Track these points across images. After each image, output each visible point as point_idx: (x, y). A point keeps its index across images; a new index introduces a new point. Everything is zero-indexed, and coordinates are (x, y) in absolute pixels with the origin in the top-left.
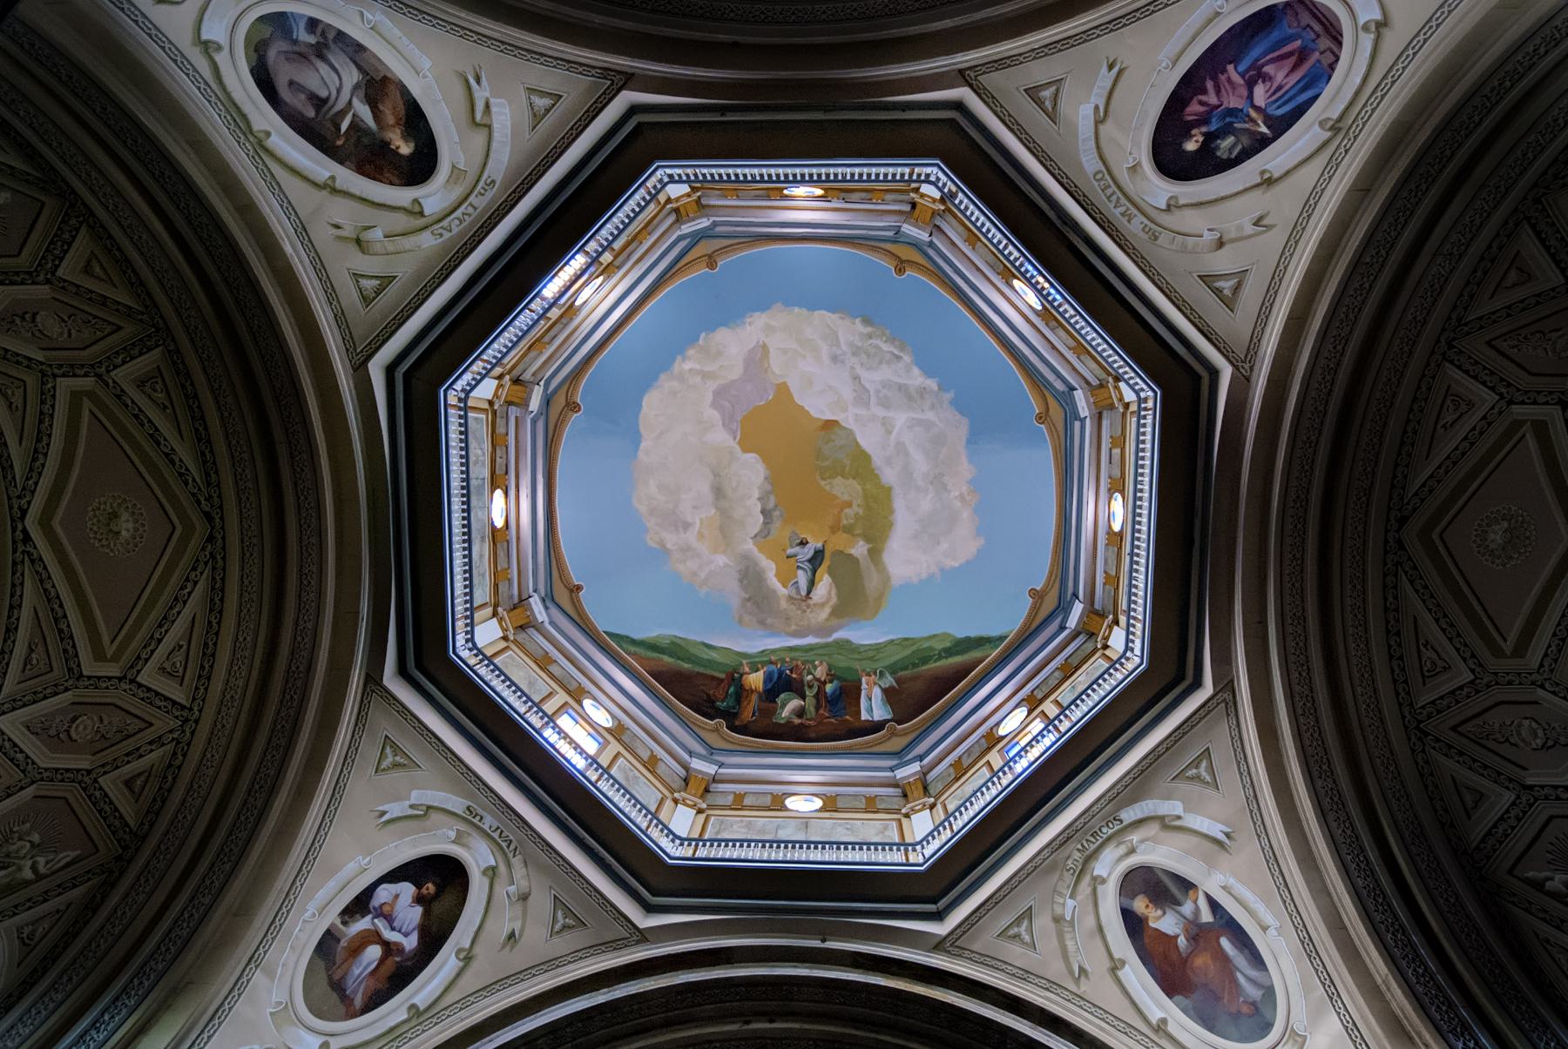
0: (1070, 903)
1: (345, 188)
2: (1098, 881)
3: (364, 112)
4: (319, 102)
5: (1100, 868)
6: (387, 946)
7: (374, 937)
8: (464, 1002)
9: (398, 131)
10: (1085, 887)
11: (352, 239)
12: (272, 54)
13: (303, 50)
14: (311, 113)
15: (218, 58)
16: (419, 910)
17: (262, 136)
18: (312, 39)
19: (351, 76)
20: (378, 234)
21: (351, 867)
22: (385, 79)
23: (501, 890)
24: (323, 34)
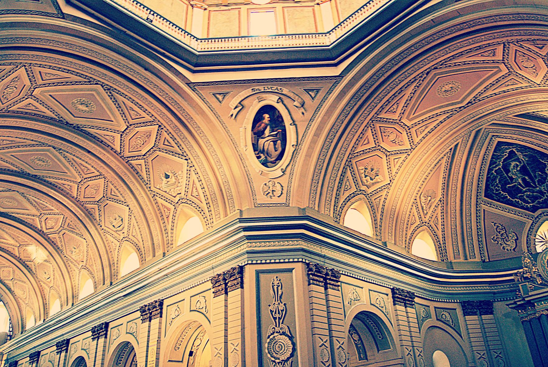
1: (291, 120)
3: (267, 132)
4: (275, 142)
9: (264, 121)
11: (304, 108)
12: (273, 159)
13: (266, 155)
14: (279, 142)
15: (284, 168)
17: (294, 146)
18: (262, 155)
19: (261, 141)
20: (296, 103)
22: (255, 134)
24: (258, 154)
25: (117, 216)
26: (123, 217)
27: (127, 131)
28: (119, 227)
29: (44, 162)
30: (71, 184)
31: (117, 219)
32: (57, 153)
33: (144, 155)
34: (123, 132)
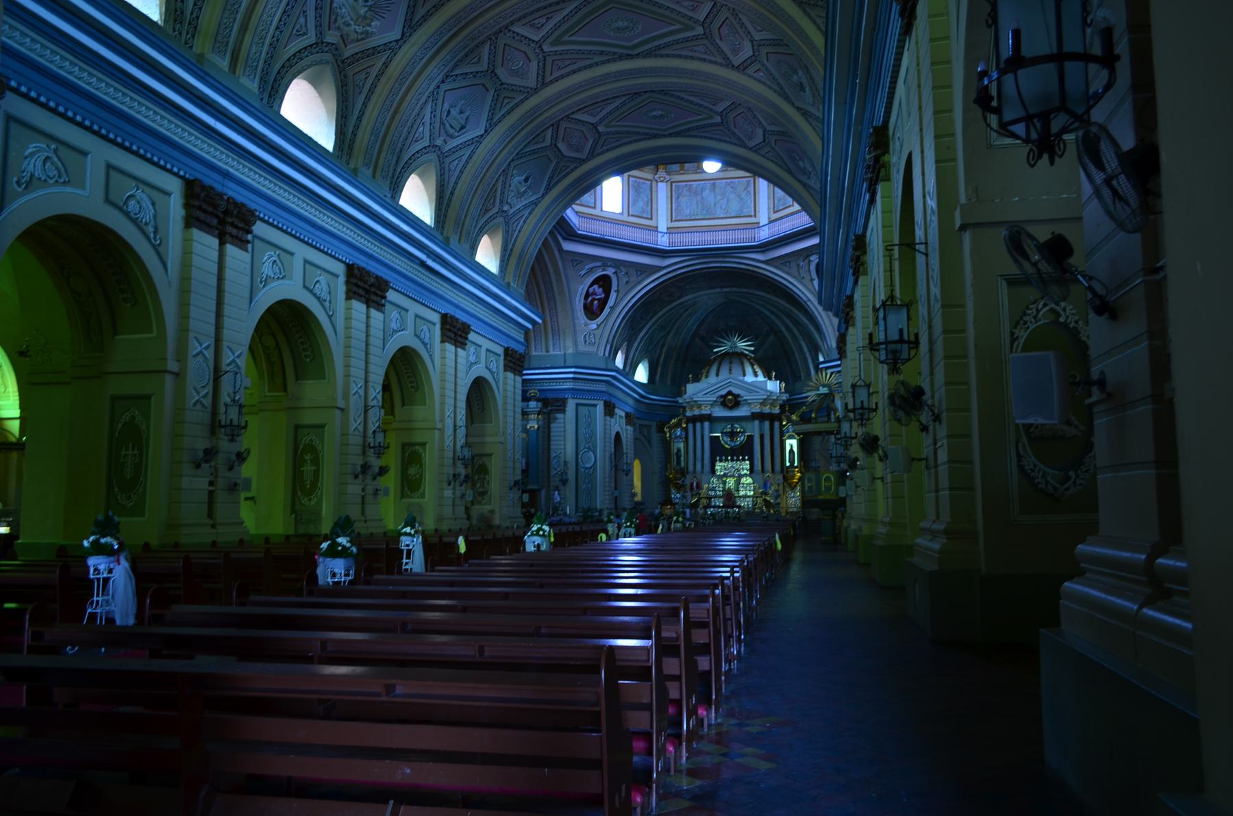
0: (802, 263)
2: (810, 261)
5: (812, 258)
6: (598, 299)
7: (594, 300)
8: (621, 300)
10: (806, 261)
16: (601, 289)
21: (580, 289)
23: (620, 275)
25: (467, 114)
26: (468, 127)
27: (594, 131)
28: (451, 126)
29: (618, 28)
30: (543, 32)
31: (462, 115)
32: (620, 51)
33: (556, 146)
34: (596, 127)
